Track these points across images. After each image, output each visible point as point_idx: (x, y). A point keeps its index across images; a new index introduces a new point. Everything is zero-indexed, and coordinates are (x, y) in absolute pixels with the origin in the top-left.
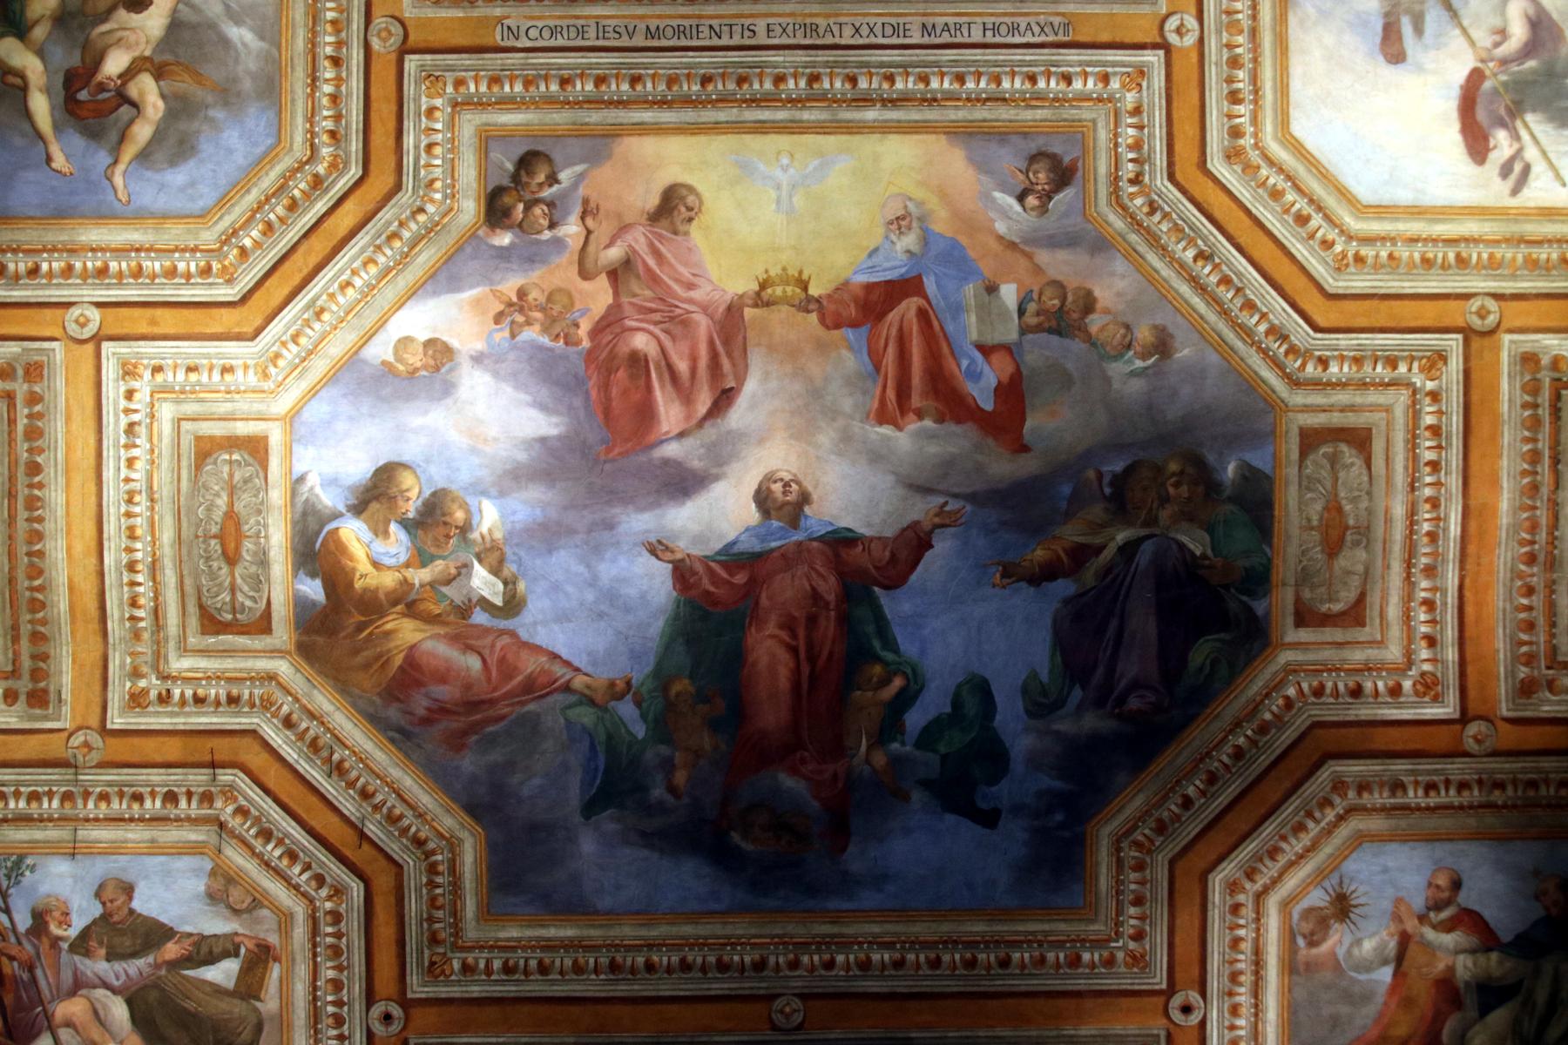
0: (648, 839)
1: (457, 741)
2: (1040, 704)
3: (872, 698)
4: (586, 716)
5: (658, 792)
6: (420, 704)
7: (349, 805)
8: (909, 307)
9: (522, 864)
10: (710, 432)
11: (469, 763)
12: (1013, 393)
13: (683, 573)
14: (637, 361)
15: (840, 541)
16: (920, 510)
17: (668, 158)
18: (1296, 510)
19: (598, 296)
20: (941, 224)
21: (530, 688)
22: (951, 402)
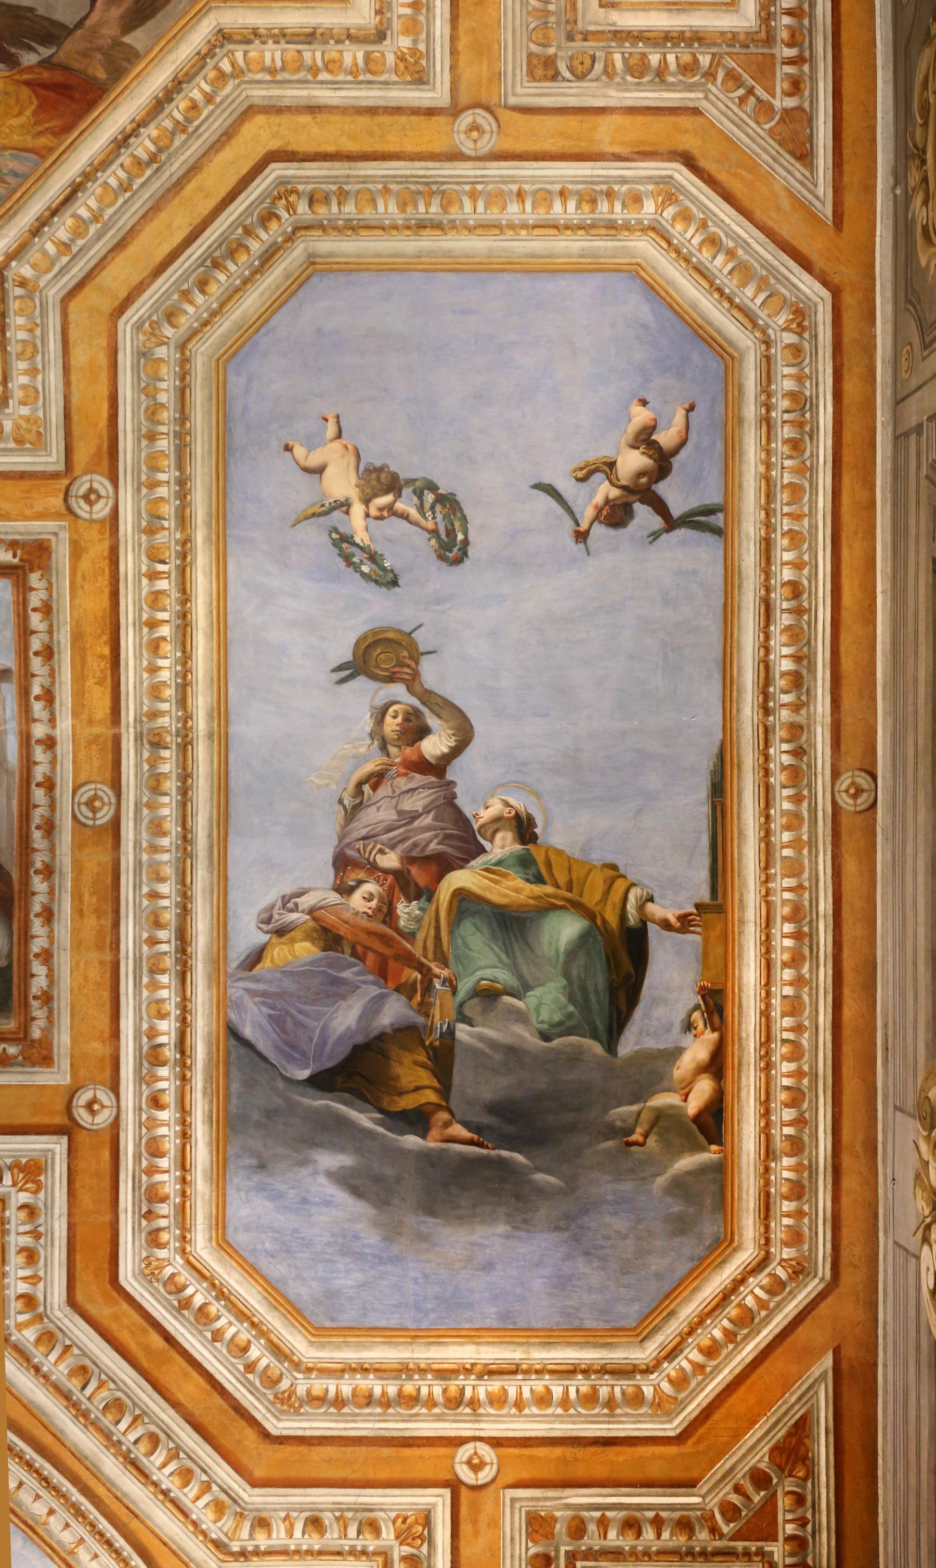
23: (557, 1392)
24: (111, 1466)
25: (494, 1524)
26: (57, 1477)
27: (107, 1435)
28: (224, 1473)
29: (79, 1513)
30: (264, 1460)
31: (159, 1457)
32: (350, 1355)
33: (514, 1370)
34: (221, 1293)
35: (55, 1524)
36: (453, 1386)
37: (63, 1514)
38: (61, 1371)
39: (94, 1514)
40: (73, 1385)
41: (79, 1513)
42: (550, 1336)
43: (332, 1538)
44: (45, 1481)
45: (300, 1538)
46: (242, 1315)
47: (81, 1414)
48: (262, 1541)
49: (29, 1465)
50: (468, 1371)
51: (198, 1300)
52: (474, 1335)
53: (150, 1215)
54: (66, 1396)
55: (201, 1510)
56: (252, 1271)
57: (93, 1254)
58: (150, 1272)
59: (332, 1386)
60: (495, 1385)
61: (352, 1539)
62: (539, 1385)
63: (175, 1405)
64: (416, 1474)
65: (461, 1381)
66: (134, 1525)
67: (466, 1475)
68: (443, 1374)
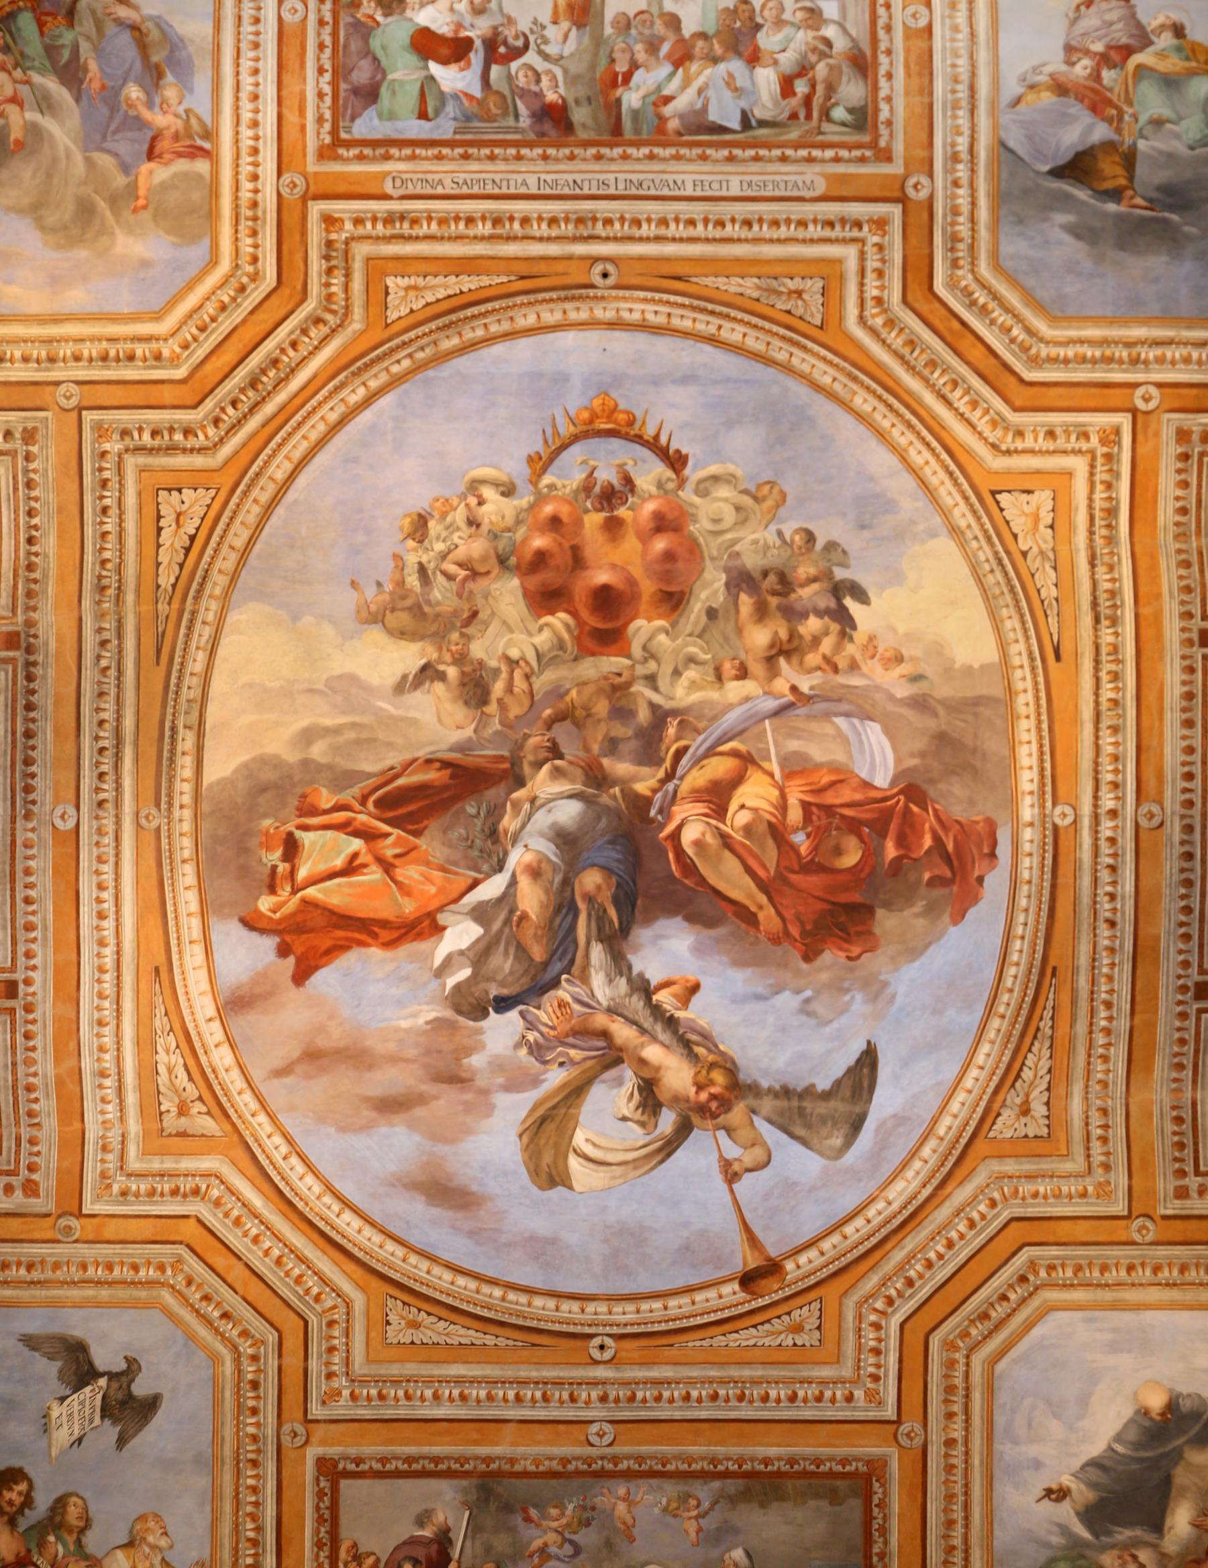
23: (1195, 355)
24: (929, 399)
25: (1157, 434)
26: (896, 404)
27: (926, 381)
28: (998, 403)
29: (910, 426)
30: (1021, 396)
31: (958, 393)
32: (1073, 333)
33: (1169, 342)
34: (995, 297)
35: (895, 433)
36: (1134, 351)
37: (901, 427)
38: (898, 343)
39: (919, 427)
40: (906, 351)
41: (910, 426)
42: (1191, 323)
43: (1061, 443)
44: (890, 407)
45: (1043, 443)
46: (1008, 310)
47: (911, 368)
48: (1020, 445)
49: (880, 398)
50: (1143, 343)
51: (982, 301)
52: (1147, 321)
53: (952, 249)
54: (901, 357)
55: (983, 425)
56: (1013, 282)
57: (918, 272)
58: (952, 284)
59: (1062, 352)
60: (1158, 351)
61: (1073, 443)
62: (1184, 351)
63: (968, 363)
64: (1111, 404)
65: (1138, 348)
66: (943, 434)
67: (1140, 405)
68: (1128, 345)
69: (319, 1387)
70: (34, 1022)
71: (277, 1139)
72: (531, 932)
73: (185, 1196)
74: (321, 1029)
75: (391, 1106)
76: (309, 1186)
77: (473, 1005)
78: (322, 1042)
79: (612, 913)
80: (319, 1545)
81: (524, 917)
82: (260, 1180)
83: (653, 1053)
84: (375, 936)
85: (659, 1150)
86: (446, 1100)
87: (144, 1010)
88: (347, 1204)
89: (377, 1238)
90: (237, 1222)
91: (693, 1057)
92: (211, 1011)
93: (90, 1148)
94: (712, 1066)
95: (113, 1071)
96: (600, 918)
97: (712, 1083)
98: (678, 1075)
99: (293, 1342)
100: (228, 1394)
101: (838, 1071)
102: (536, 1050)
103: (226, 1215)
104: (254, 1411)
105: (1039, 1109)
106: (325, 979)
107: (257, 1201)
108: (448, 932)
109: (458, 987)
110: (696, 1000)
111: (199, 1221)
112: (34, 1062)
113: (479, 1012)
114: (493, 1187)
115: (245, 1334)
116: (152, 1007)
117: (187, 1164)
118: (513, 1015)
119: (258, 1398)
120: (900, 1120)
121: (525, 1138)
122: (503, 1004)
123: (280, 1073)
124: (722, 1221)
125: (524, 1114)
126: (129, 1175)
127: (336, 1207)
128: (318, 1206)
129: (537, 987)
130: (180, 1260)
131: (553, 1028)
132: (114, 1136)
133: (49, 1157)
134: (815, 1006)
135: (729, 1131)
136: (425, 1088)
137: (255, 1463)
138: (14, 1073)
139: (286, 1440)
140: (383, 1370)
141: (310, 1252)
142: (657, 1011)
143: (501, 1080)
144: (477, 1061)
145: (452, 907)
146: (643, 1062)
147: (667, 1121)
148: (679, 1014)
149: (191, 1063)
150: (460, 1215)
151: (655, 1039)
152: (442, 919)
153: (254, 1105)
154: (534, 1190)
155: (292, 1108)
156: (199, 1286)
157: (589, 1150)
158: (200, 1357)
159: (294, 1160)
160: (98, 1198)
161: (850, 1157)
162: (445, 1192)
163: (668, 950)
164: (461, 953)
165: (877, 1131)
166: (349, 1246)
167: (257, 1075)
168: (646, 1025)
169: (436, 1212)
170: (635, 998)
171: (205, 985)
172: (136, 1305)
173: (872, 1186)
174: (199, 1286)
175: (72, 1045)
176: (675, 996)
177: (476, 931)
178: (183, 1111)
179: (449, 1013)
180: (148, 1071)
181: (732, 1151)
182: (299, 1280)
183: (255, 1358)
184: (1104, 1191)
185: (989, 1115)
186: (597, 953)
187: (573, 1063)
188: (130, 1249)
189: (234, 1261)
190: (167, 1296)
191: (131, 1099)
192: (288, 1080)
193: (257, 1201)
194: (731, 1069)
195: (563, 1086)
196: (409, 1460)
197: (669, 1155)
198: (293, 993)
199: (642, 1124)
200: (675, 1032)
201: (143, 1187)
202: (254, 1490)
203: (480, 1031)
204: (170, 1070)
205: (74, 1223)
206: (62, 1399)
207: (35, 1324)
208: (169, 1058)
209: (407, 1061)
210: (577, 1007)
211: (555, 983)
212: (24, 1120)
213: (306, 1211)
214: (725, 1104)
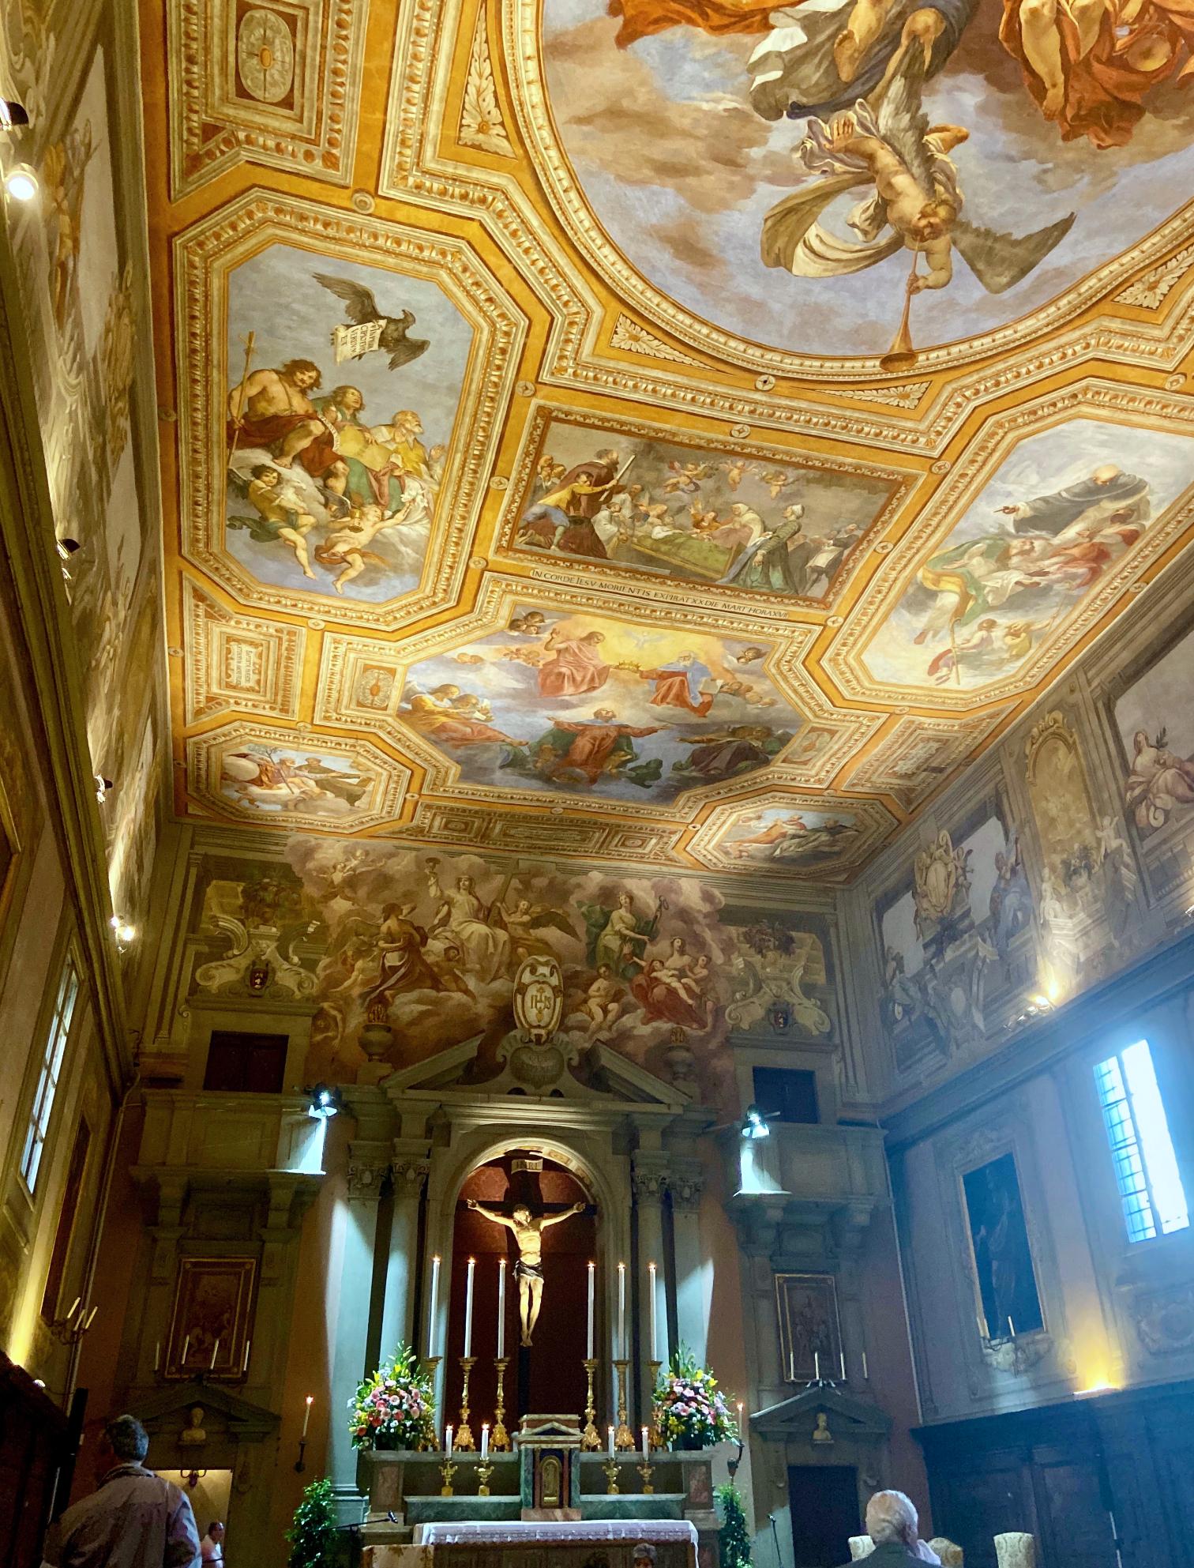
0: (521, 775)
1: (457, 747)
2: (677, 767)
3: (617, 759)
4: (509, 748)
5: (530, 766)
6: (444, 736)
7: (411, 756)
8: (678, 679)
9: (472, 771)
10: (583, 695)
11: (459, 752)
12: (707, 706)
13: (557, 724)
14: (561, 675)
15: (621, 727)
16: (656, 724)
17: (597, 624)
18: (795, 745)
19: (553, 655)
20: (702, 660)
21: (489, 739)
22: (681, 700)
69: (551, 363)
70: (348, 12)
71: (562, 173)
72: (849, 52)
73: (472, 202)
74: (630, 93)
75: (669, 170)
76: (581, 219)
77: (770, 104)
78: (626, 103)
79: (928, 55)
80: (527, 454)
81: (849, 37)
82: (540, 206)
83: (901, 181)
84: (705, 16)
85: (870, 256)
86: (715, 180)
87: (466, 31)
88: (608, 240)
89: (626, 273)
90: (514, 234)
91: (931, 191)
92: (530, 50)
93: (390, 139)
94: (944, 202)
95: (424, 79)
96: (915, 56)
97: (935, 214)
98: (911, 201)
99: (539, 329)
100: (481, 353)
101: (1036, 228)
102: (809, 157)
103: (506, 226)
104: (499, 368)
105: (1163, 288)
106: (648, 46)
107: (535, 222)
108: (776, 31)
109: (764, 85)
110: (959, 149)
111: (481, 225)
112: (346, 51)
113: (774, 113)
114: (730, 255)
115: (503, 316)
116: (474, 31)
117: (477, 174)
118: (802, 122)
119: (503, 360)
120: (1059, 273)
121: (769, 223)
122: (797, 111)
123: (580, 120)
124: (891, 318)
125: (776, 202)
126: (424, 173)
127: (599, 242)
128: (585, 238)
129: (834, 102)
130: (460, 251)
131: (831, 142)
132: (413, 134)
133: (349, 134)
134: (1050, 179)
135: (929, 253)
136: (703, 163)
137: (492, 399)
138: (323, 55)
139: (519, 390)
140: (603, 362)
141: (569, 270)
142: (922, 148)
143: (768, 172)
144: (756, 152)
145: (787, 9)
146: (890, 185)
147: (886, 235)
148: (939, 156)
149: (501, 92)
150: (697, 270)
151: (909, 171)
152: (773, 18)
153: (549, 141)
154: (762, 265)
155: (583, 152)
156: (473, 274)
157: (816, 244)
158: (465, 324)
159: (573, 195)
160: (393, 186)
161: (1007, 294)
162: (689, 248)
163: (959, 101)
164: (779, 54)
165: (1038, 277)
166: (601, 273)
167: (560, 117)
168: (907, 158)
169: (678, 263)
170: (910, 133)
171: (530, 25)
172: (417, 275)
173: (1009, 317)
174: (473, 274)
175: (387, 46)
176: (943, 140)
177: (802, 38)
178: (482, 128)
179: (748, 107)
180: (458, 90)
181: (923, 268)
182: (554, 288)
183: (507, 334)
184: (1167, 354)
185: (1126, 284)
186: (898, 86)
187: (833, 173)
188: (418, 233)
189: (506, 262)
190: (444, 275)
191: (436, 107)
192: (586, 128)
193: (535, 222)
194: (955, 207)
195: (818, 189)
196: (603, 420)
197: (875, 262)
198: (615, 54)
199: (865, 233)
200: (927, 170)
201: (436, 186)
202: (489, 415)
203: (769, 129)
204: (479, 93)
205: (369, 199)
206: (348, 327)
207: (327, 270)
208: (481, 81)
209: (697, 138)
210: (858, 129)
211: (849, 104)
212: (327, 98)
213: (574, 239)
214: (936, 232)
